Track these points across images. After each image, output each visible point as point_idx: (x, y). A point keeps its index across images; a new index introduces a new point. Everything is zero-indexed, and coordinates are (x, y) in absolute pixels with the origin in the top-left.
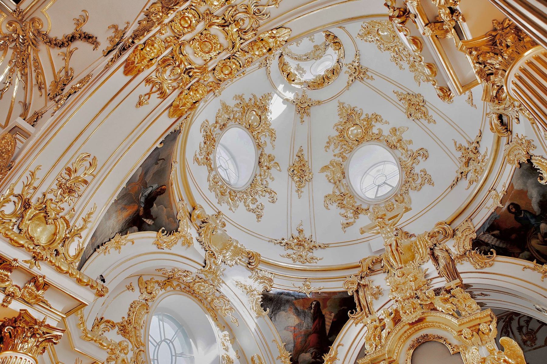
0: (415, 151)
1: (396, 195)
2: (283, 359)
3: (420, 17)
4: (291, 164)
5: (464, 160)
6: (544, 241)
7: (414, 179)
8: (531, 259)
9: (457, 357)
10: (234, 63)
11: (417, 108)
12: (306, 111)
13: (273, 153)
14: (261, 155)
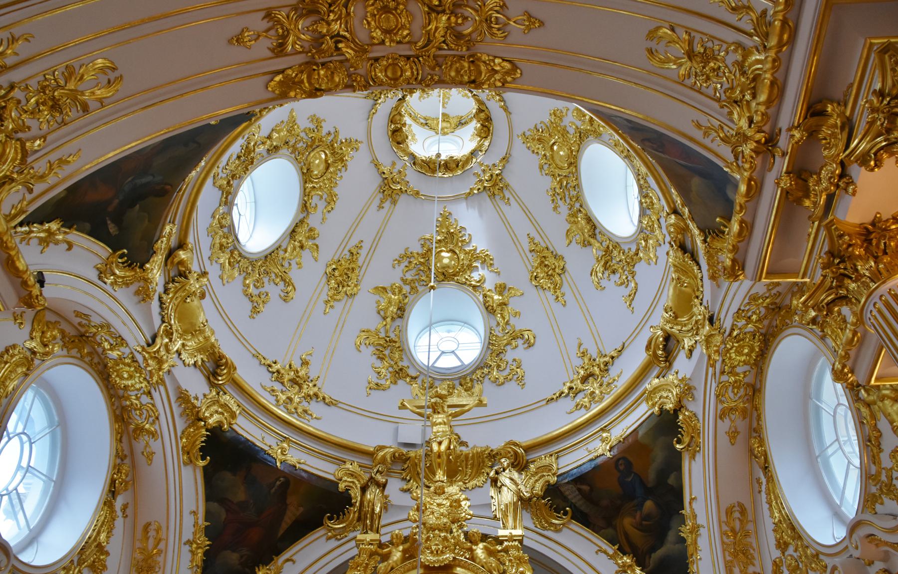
0: (517, 329)
1: (465, 377)
2: (194, 546)
3: (787, 158)
4: (336, 258)
5: (582, 372)
7: (499, 366)
8: (612, 542)
10: (412, 68)
11: (550, 273)
12: (394, 196)
13: (319, 229)
14: (302, 221)
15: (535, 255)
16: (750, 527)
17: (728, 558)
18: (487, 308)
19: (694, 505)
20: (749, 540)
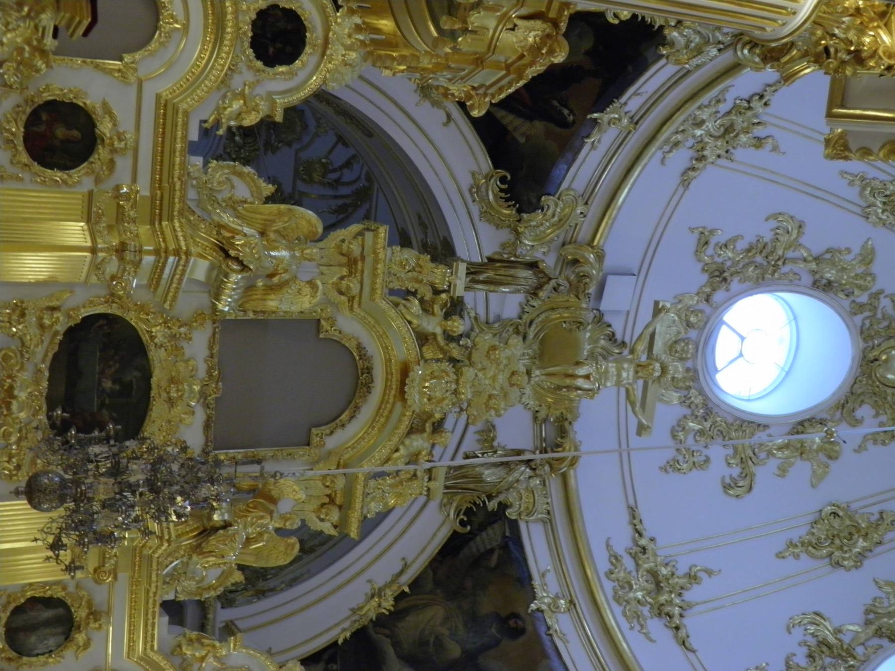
5: (664, 571)
8: (415, 585)
11: (837, 541)
15: (874, 518)
18: (801, 423)
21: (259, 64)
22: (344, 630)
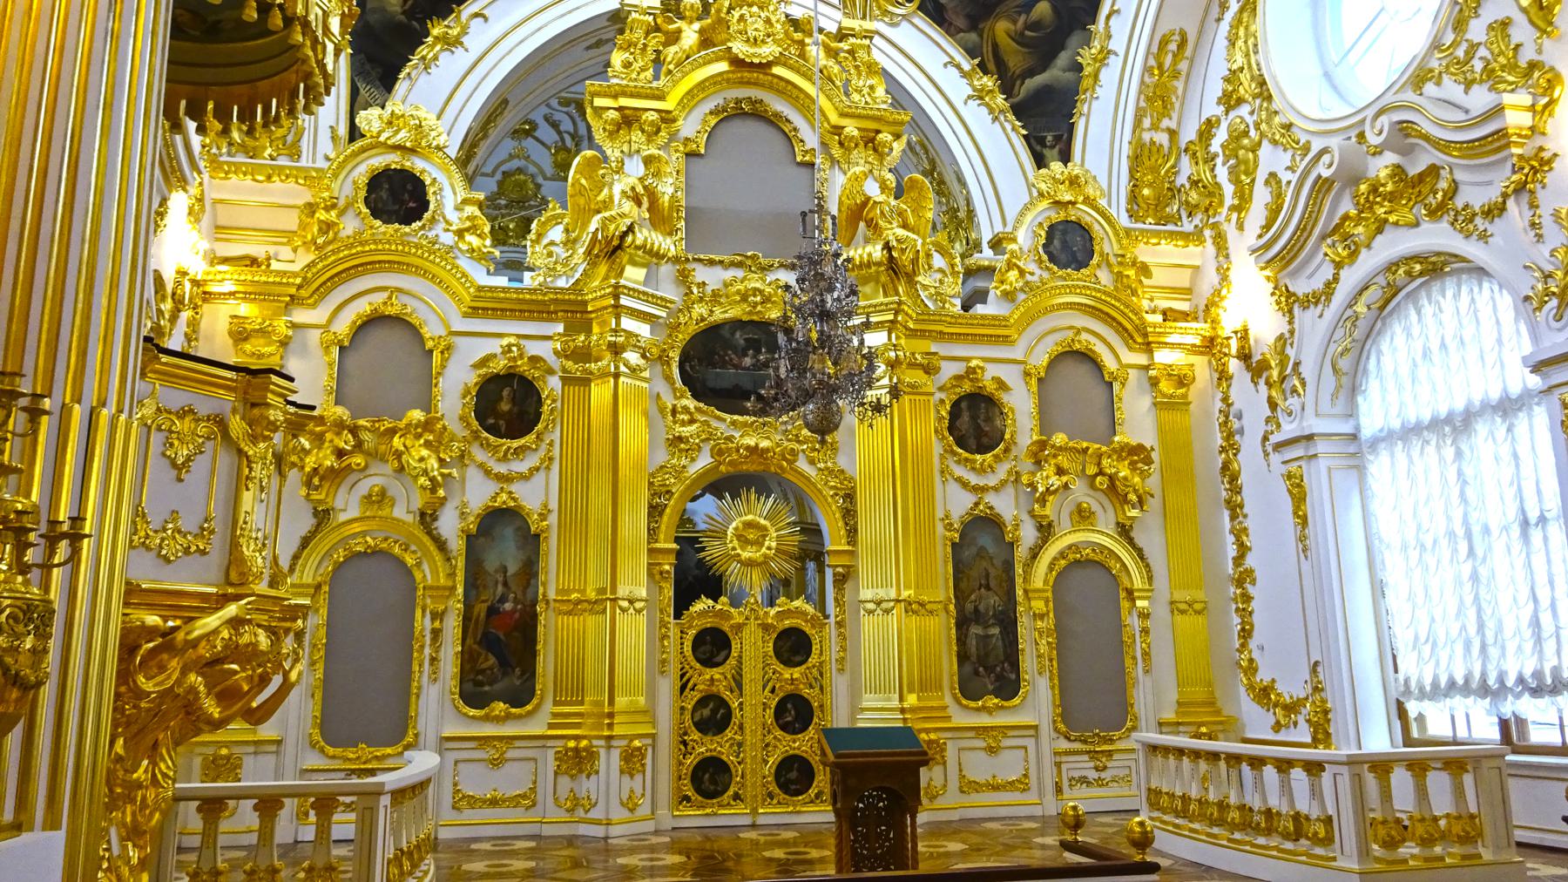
6: (1022, 34)
8: (971, 52)
9: (804, 170)
16: (1183, 66)
17: (1142, 104)
19: (1112, 22)
20: (1175, 83)
21: (427, 215)
22: (1013, 129)
